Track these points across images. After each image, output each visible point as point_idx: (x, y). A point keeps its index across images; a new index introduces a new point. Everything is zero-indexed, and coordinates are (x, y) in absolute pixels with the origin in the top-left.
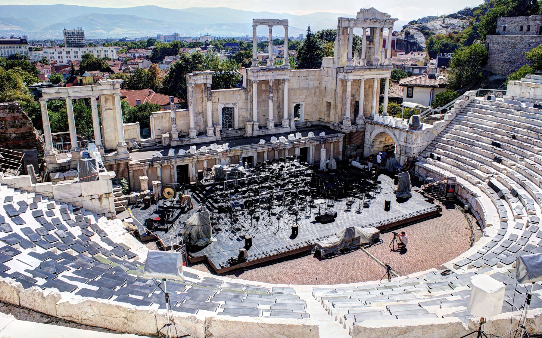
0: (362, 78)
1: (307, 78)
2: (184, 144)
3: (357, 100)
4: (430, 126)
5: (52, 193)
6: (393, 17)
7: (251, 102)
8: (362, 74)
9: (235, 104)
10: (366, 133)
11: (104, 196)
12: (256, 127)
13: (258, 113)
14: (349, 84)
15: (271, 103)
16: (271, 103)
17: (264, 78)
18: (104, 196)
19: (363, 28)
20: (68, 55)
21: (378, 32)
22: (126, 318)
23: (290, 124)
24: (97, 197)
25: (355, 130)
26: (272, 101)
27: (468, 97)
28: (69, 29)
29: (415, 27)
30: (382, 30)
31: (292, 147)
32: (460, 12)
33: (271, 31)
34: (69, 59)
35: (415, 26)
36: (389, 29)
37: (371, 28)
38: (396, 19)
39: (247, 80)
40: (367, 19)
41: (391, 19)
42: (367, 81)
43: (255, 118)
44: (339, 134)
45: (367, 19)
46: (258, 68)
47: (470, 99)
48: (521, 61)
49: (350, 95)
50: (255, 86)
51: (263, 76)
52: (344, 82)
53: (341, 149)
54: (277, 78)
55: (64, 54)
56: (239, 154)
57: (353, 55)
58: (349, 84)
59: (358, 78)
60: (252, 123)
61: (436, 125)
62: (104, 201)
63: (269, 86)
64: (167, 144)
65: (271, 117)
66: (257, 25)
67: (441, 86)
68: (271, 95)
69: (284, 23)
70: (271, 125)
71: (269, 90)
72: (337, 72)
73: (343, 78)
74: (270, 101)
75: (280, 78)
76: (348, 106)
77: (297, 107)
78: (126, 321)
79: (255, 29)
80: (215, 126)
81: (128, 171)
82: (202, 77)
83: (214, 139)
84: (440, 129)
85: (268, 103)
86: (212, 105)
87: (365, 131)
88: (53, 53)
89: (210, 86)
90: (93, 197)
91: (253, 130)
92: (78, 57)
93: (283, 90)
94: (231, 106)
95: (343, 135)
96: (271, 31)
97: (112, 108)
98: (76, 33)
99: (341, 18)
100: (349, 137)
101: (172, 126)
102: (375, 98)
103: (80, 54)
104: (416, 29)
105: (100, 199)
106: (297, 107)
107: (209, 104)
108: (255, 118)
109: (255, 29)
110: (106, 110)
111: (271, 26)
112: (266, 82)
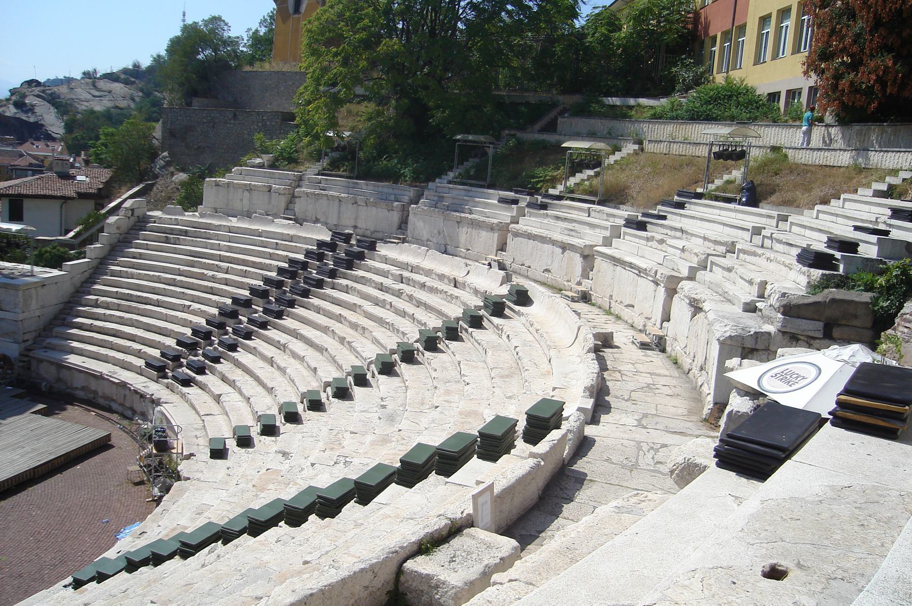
4: (56, 272)
29: (37, 93)
32: (125, 71)
35: (37, 90)
47: (136, 214)
48: (225, 147)
61: (68, 269)
67: (82, 196)
84: (78, 279)
104: (38, 96)
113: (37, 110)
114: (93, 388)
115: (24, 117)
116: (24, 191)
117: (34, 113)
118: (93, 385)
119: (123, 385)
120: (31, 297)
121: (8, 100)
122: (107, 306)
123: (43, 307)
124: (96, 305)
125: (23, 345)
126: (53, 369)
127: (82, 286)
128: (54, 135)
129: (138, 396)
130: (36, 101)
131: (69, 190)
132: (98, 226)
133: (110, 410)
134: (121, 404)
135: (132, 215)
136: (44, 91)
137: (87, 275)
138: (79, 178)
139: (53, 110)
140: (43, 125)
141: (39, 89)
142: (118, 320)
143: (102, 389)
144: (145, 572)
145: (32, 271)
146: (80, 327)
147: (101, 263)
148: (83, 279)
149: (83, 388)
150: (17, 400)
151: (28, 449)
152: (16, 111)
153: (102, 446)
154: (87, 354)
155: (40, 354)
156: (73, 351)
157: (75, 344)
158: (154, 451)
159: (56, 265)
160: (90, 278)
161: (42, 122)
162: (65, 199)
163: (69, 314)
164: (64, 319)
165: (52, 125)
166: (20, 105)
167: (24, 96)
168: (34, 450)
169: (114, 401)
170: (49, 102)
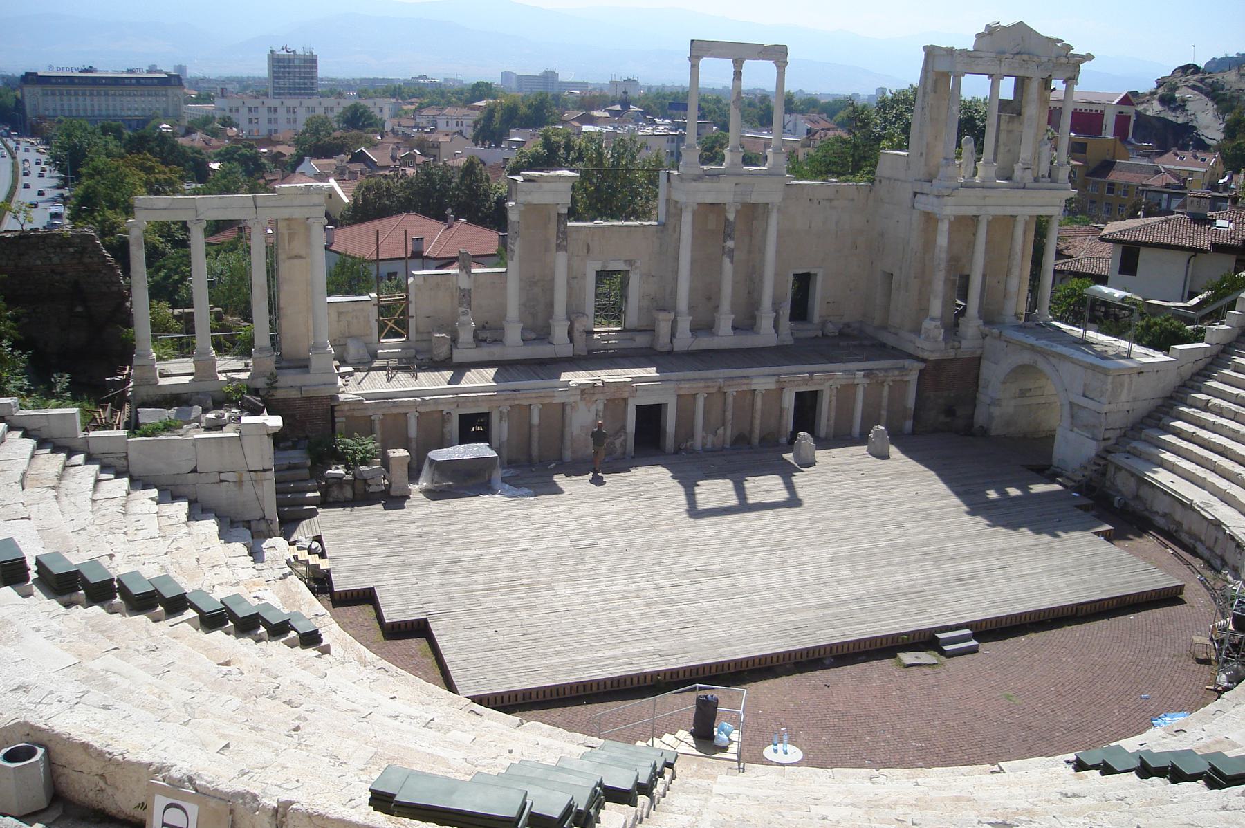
1: (835, 203)
3: (966, 272)
4: (1160, 357)
5: (126, 457)
6: (1077, 50)
7: (677, 259)
9: (630, 262)
10: (984, 363)
12: (684, 324)
13: (692, 291)
14: (944, 227)
15: (727, 265)
16: (727, 265)
17: (710, 199)
19: (990, 76)
21: (1034, 88)
22: (102, 776)
23: (776, 326)
25: (951, 354)
26: (732, 262)
29: (1192, 82)
30: (1047, 83)
31: (773, 386)
33: (738, 75)
34: (273, 127)
35: (1193, 80)
36: (1065, 82)
37: (1017, 78)
38: (1089, 57)
39: (668, 200)
40: (1004, 53)
41: (1074, 55)
42: (995, 221)
43: (683, 303)
44: (907, 363)
45: (1004, 53)
46: (697, 172)
49: (943, 255)
50: (687, 218)
51: (708, 193)
52: (930, 220)
53: (911, 402)
55: (263, 114)
56: (626, 395)
57: (959, 145)
58: (944, 227)
59: (972, 211)
60: (672, 316)
61: (1177, 355)
62: (248, 486)
63: (727, 219)
64: (443, 356)
65: (726, 305)
66: (699, 58)
67: (1218, 248)
68: (730, 244)
69: (777, 54)
70: (725, 323)
71: (727, 231)
72: (915, 194)
73: (929, 209)
74: (727, 261)
76: (939, 285)
77: (803, 282)
78: (102, 783)
79: (694, 68)
80: (573, 317)
81: (333, 418)
82: (546, 186)
83: (565, 350)
84: (1188, 369)
85: (721, 267)
86: (569, 260)
87: (980, 358)
88: (237, 111)
89: (565, 211)
90: (223, 477)
91: (673, 335)
92: (295, 122)
93: (765, 231)
94: (620, 266)
95: (922, 365)
96: (738, 75)
97: (302, 253)
98: (297, 63)
99: (933, 47)
100: (933, 373)
101: (461, 309)
102: (1016, 271)
103: (302, 117)
104: (1194, 87)
106: (803, 282)
107: (561, 259)
108: (683, 303)
109: (694, 68)
110: (290, 258)
111: (738, 63)
113: (1189, 106)
114: (1178, 518)
115: (1170, 116)
116: (1142, 238)
117: (1184, 110)
118: (1179, 515)
119: (1217, 524)
120: (1122, 385)
121: (1152, 94)
122: (1220, 412)
123: (1135, 400)
124: (1206, 407)
125: (1103, 444)
126: (1132, 482)
127: (1191, 379)
128: (1208, 142)
129: (1234, 545)
130: (1190, 94)
131: (1201, 238)
132: (1230, 299)
133: (1193, 552)
134: (1208, 548)
136: (1202, 81)
137: (1201, 364)
138: (1219, 223)
139: (1211, 106)
140: (1194, 128)
141: (1196, 77)
142: (1231, 434)
143: (1188, 522)
144: (1157, 784)
145: (1130, 351)
146: (1179, 434)
147: (1223, 351)
148: (1194, 370)
149: (1165, 515)
150: (1080, 512)
151: (1076, 578)
152: (1160, 108)
153: (1169, 597)
154: (1180, 471)
155: (1119, 459)
156: (1163, 464)
157: (1167, 456)
158: (1231, 628)
159: (1163, 347)
160: (1205, 369)
161: (1194, 124)
162: (1195, 251)
163: (1167, 414)
164: (1160, 420)
165: (1207, 127)
166: (1168, 101)
167: (1175, 88)
168: (1085, 581)
169: (1201, 541)
170: (1207, 95)
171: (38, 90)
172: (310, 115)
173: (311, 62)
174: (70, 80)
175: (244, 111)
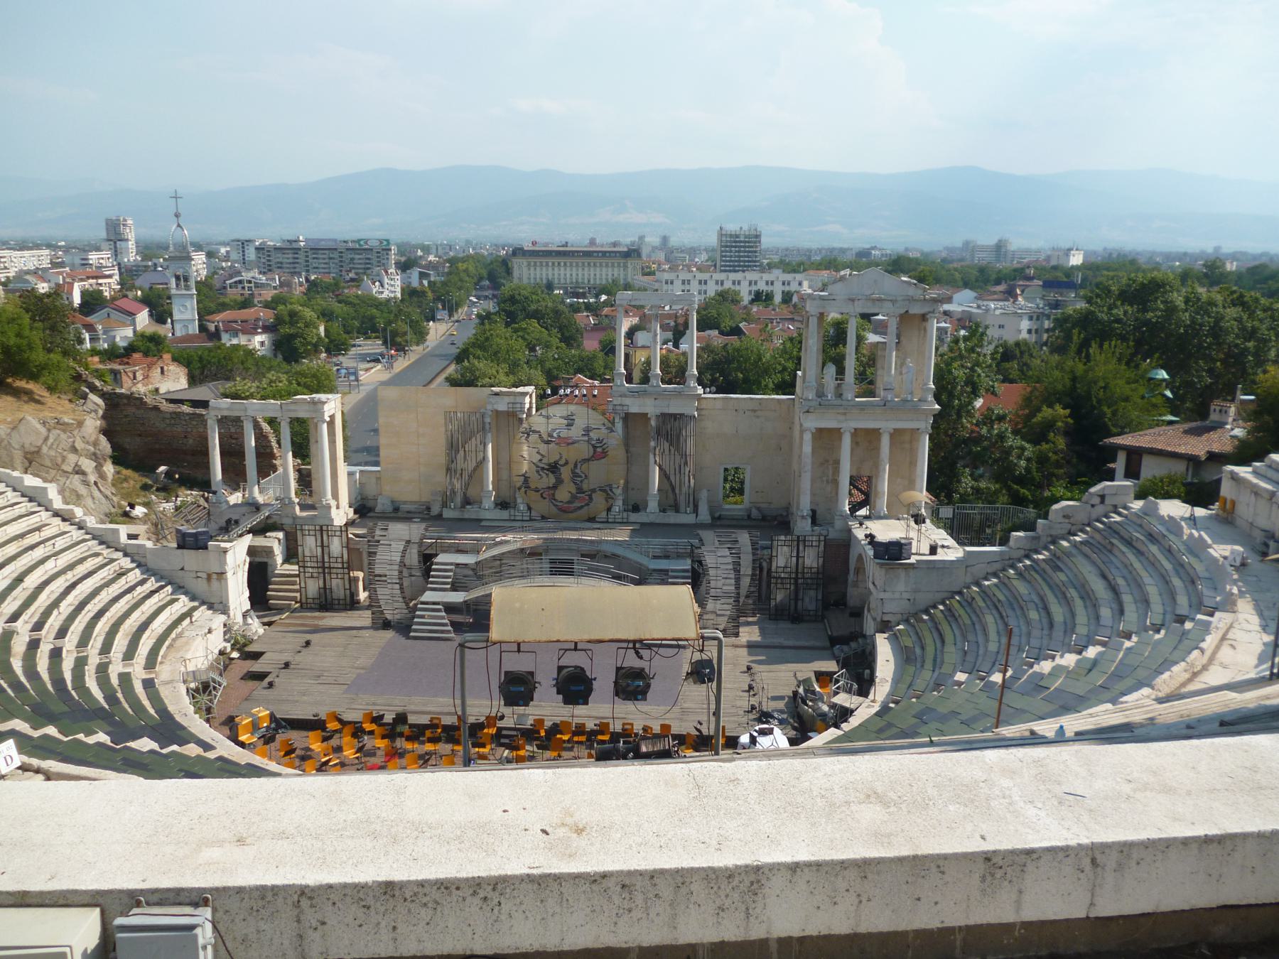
0: (843, 425)
1: (759, 413)
2: (466, 516)
8: (842, 418)
11: (215, 576)
17: (634, 409)
18: (215, 576)
20: (704, 287)
24: (204, 575)
27: (1102, 498)
28: (732, 227)
47: (1108, 501)
54: (666, 411)
70: (653, 505)
75: (673, 410)
103: (712, 290)
105: (209, 577)
112: (644, 417)
123: (916, 591)
135: (1102, 502)
171: (524, 262)
172: (720, 288)
173: (753, 239)
174: (548, 254)
175: (678, 283)
